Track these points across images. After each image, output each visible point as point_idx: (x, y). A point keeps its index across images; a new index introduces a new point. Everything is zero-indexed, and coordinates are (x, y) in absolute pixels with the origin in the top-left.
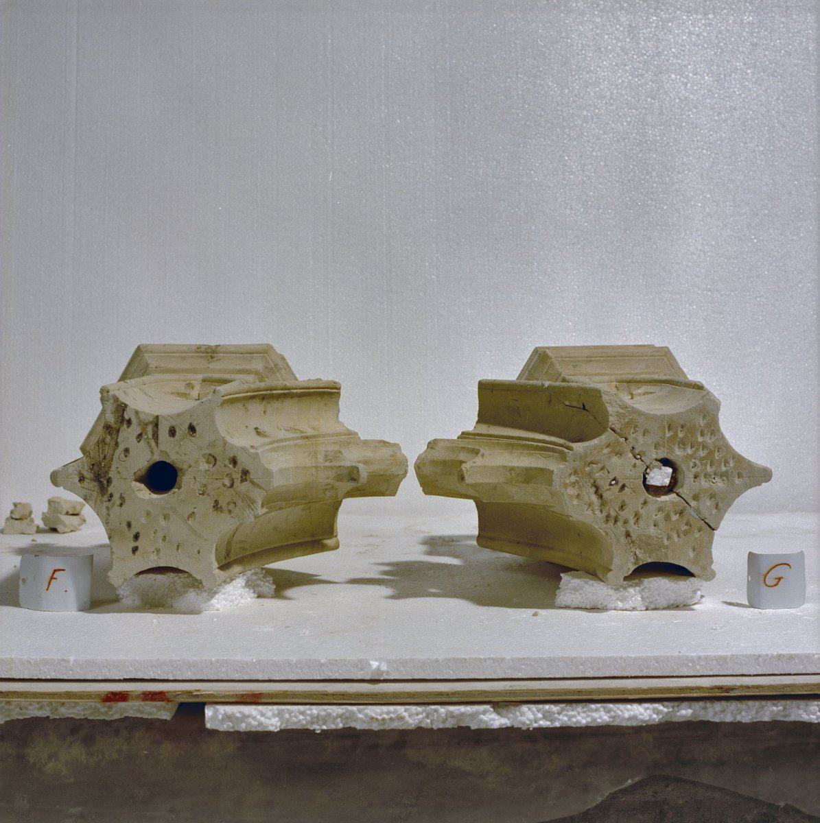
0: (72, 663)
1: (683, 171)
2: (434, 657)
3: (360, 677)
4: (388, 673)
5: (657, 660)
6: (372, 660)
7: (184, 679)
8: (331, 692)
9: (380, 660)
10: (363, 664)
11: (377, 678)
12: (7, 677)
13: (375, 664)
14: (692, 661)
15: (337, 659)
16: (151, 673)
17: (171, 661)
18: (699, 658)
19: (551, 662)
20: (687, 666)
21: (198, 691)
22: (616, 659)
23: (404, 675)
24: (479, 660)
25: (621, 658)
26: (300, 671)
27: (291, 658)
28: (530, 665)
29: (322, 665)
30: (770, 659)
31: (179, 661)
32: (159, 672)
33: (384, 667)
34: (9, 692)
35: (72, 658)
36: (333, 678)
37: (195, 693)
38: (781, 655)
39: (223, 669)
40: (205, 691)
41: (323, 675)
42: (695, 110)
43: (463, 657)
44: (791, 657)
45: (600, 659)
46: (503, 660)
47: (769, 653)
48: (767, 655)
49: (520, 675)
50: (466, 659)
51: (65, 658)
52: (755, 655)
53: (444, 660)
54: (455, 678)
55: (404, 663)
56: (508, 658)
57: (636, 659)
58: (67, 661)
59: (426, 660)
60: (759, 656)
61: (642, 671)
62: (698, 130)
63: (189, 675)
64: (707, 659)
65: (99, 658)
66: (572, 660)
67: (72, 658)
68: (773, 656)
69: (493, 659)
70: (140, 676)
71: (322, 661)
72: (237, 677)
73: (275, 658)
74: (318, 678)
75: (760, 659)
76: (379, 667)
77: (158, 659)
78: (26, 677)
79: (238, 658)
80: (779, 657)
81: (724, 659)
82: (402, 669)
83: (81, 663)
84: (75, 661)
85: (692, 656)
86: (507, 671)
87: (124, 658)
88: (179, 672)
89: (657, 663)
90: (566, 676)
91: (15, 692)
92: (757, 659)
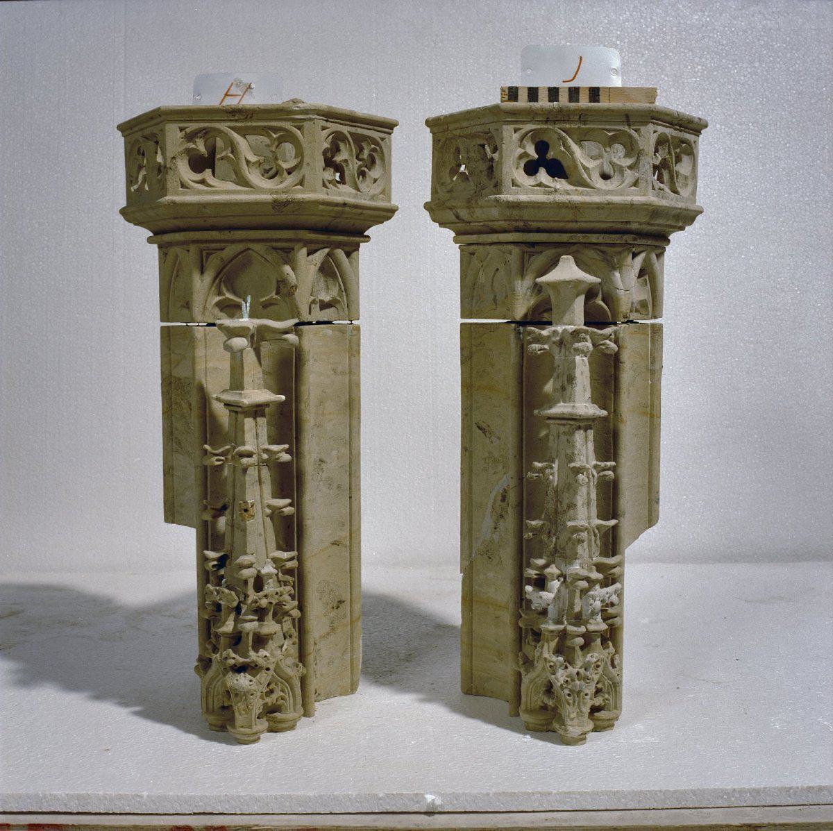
0: (145, 797)
1: (727, 223)
2: (485, 792)
3: (416, 810)
4: (442, 806)
5: (694, 792)
6: (427, 793)
7: (251, 813)
8: (381, 828)
9: (434, 793)
10: (419, 797)
11: (432, 811)
12: (84, 811)
13: (430, 798)
14: (727, 794)
15: (395, 793)
16: (220, 808)
17: (238, 796)
18: (734, 790)
19: (595, 795)
20: (722, 798)
21: (257, 825)
22: (656, 793)
23: (457, 808)
24: (528, 794)
25: (661, 792)
26: (359, 805)
27: (350, 793)
28: (576, 798)
29: (380, 799)
30: (801, 791)
31: (246, 796)
32: (227, 807)
33: (438, 802)
34: (81, 825)
35: (145, 794)
36: (391, 810)
37: (253, 828)
38: (810, 787)
39: (288, 804)
40: (263, 826)
41: (381, 808)
42: (739, 161)
43: (513, 791)
44: (820, 789)
45: (641, 792)
46: (550, 793)
47: (799, 785)
48: (798, 788)
49: (565, 808)
50: (515, 793)
51: (139, 794)
52: (785, 788)
53: (495, 794)
54: (504, 810)
55: (456, 797)
56: (555, 791)
57: (675, 792)
58: (141, 797)
59: (478, 794)
60: (791, 788)
61: (681, 803)
62: (743, 180)
63: (255, 809)
64: (742, 791)
65: (170, 793)
66: (615, 793)
67: (145, 794)
68: (803, 789)
69: (540, 793)
70: (209, 810)
71: (381, 795)
72: (300, 810)
73: (335, 793)
74: (377, 811)
75: (792, 791)
76: (433, 800)
77: (226, 795)
78: (102, 811)
79: (302, 793)
80: (809, 789)
81: (758, 791)
82: (456, 802)
83: (153, 798)
84: (148, 796)
85: (727, 790)
86: (553, 804)
87: (193, 793)
88: (246, 807)
89: (694, 796)
90: (608, 808)
91: (87, 825)
92: (787, 791)
